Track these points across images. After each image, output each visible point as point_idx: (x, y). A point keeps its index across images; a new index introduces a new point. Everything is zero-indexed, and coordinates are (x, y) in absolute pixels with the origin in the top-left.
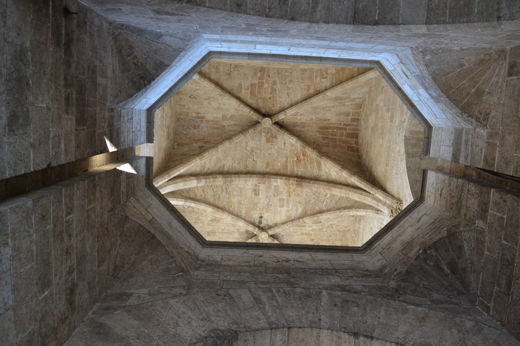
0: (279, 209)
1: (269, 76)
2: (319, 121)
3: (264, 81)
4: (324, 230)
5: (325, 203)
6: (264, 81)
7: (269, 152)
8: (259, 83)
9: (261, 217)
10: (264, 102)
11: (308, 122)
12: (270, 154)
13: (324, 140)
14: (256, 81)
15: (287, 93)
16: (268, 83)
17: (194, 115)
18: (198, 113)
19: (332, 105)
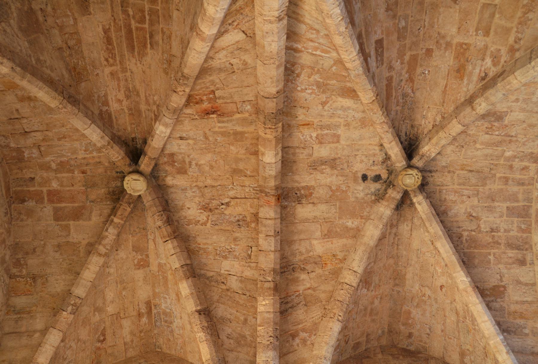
0: (342, 142)
1: (32, 179)
2: (114, 57)
3: (45, 190)
4: (403, 23)
5: (318, 53)
6: (45, 190)
7: (207, 168)
8: (51, 201)
9: (365, 178)
10: (94, 185)
11: (122, 83)
12: (212, 167)
13: (157, 43)
14: (48, 210)
15: (59, 139)
16: (47, 181)
17: (144, 320)
18: (140, 315)
19: (56, 32)
